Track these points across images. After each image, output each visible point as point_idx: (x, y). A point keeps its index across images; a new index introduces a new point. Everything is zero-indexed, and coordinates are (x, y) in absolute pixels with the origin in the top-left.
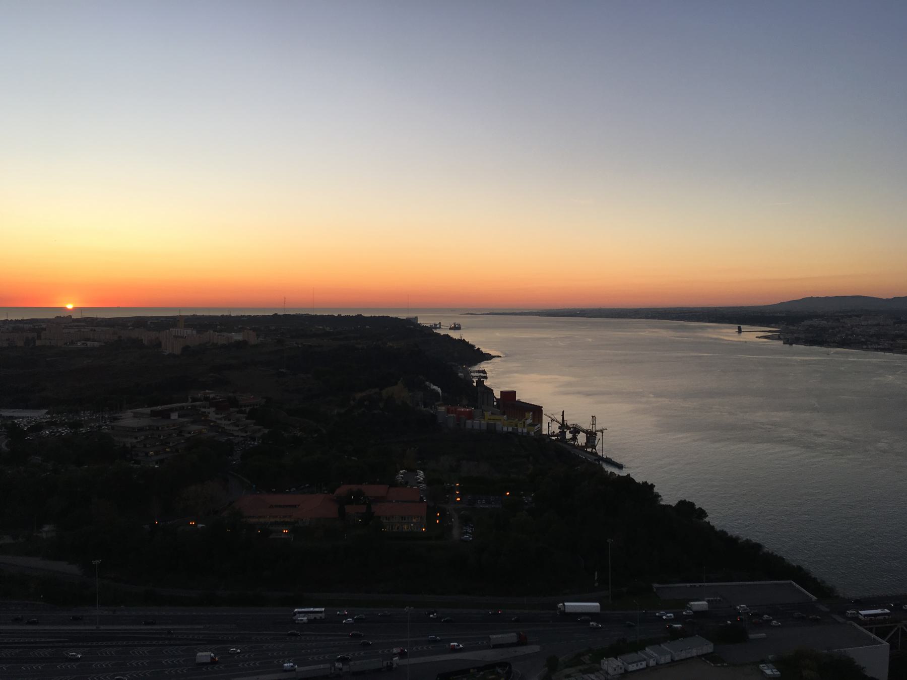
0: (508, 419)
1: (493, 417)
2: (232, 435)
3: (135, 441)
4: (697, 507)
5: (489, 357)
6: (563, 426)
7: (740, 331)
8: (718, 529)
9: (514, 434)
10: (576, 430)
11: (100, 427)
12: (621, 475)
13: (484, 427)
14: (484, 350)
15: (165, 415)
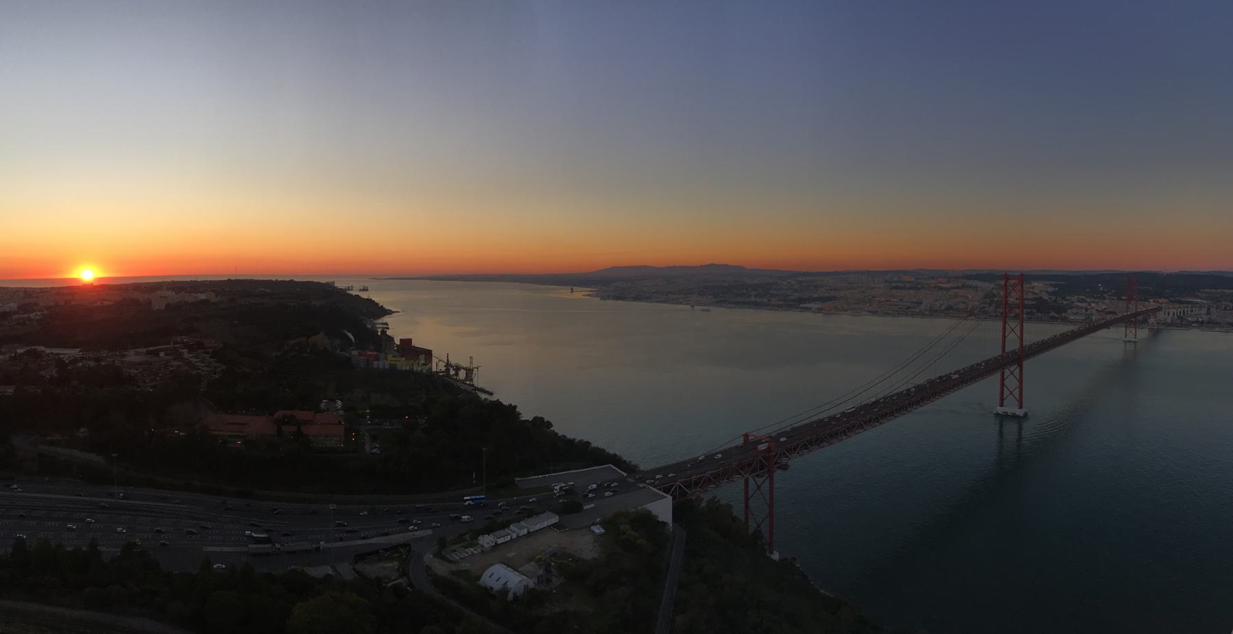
0: (406, 360)
1: (395, 359)
2: (200, 369)
3: (136, 372)
4: (546, 420)
5: (389, 312)
6: (448, 365)
7: (572, 292)
8: (560, 434)
9: (411, 371)
10: (458, 369)
11: (114, 361)
12: (492, 400)
13: (387, 367)
14: (387, 307)
15: (156, 353)
